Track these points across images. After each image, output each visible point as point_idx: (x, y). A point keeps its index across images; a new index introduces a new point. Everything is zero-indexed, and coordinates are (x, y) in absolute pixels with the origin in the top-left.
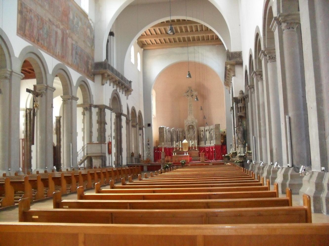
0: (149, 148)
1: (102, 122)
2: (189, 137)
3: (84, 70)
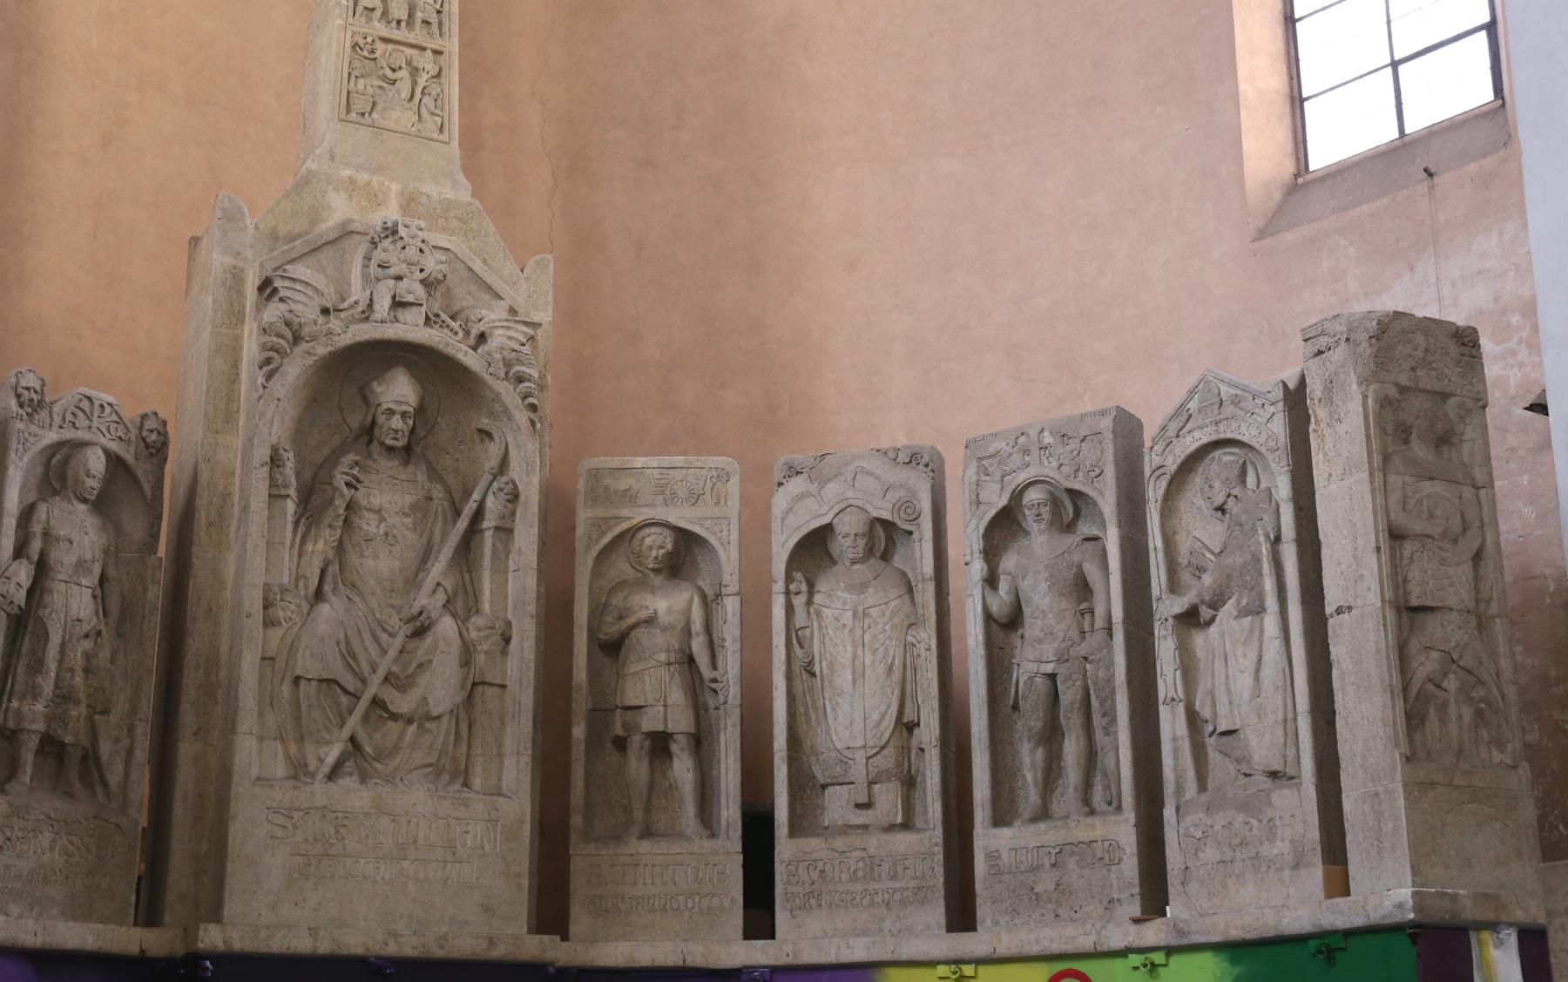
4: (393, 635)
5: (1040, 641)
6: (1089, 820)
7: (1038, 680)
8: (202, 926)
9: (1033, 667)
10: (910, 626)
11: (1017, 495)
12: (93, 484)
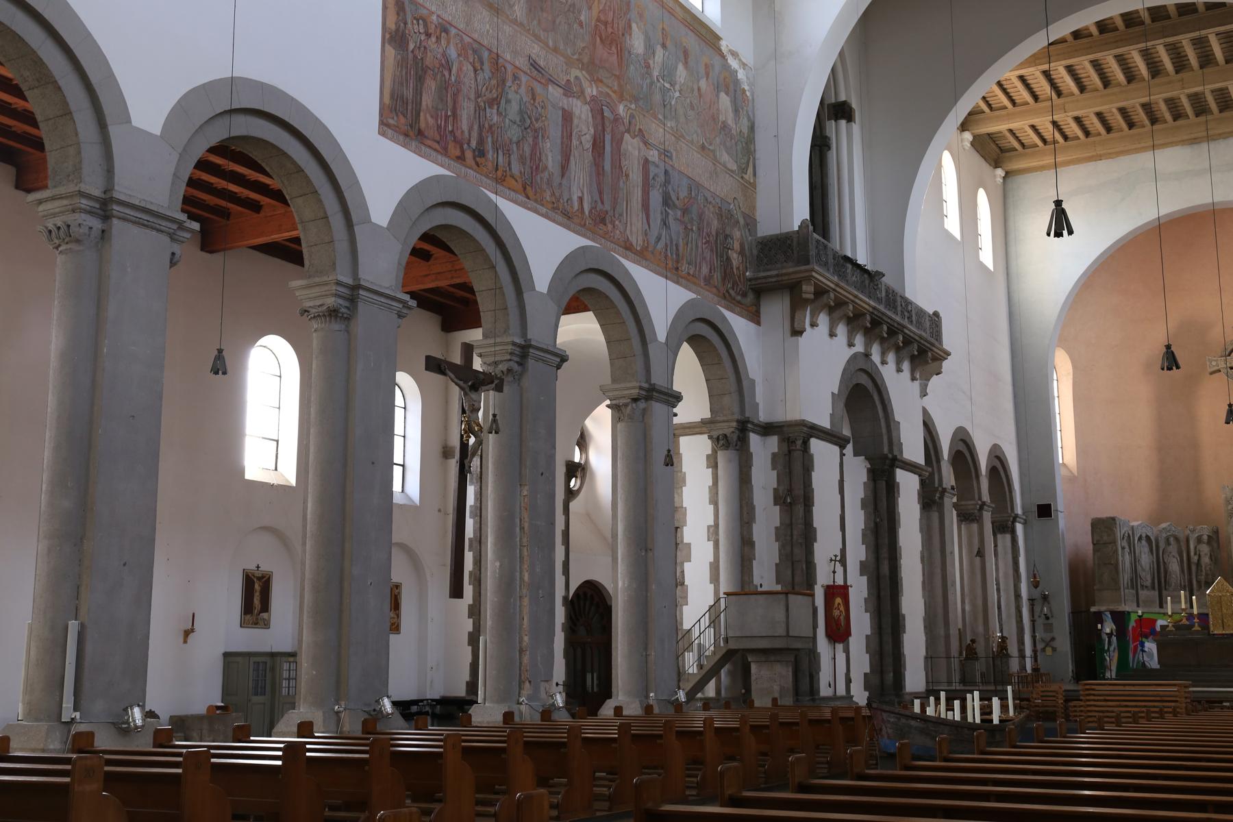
0: (1047, 618)
1: (795, 497)
3: (705, 270)
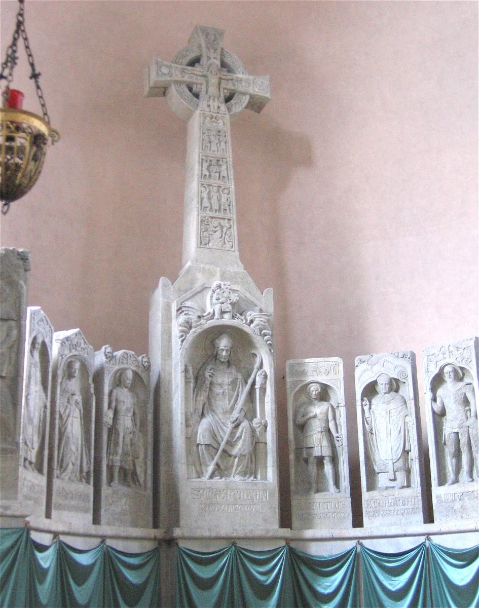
2: (202, 435)
4: (227, 427)
5: (452, 421)
6: (472, 483)
7: (452, 434)
8: (174, 528)
9: (450, 430)
10: (406, 416)
11: (442, 369)
12: (129, 382)
